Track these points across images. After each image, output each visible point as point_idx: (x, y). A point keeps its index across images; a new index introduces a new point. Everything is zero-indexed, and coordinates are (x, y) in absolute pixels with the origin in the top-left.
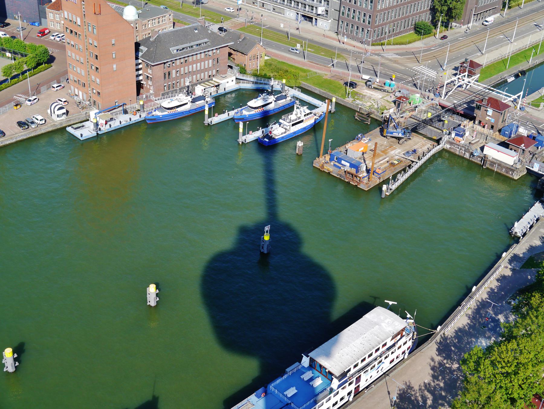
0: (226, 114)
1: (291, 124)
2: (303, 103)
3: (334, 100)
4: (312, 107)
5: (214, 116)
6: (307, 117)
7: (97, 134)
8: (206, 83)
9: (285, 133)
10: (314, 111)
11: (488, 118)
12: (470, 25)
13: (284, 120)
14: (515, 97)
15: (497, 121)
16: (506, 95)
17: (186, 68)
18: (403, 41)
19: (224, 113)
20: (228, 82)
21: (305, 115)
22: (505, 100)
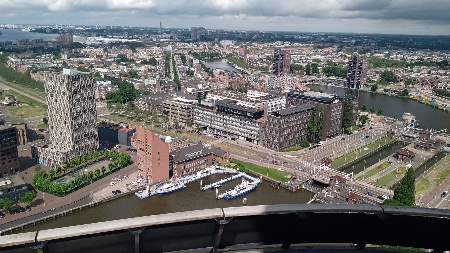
0: (211, 185)
1: (240, 189)
2: (246, 179)
3: (261, 177)
4: (251, 181)
5: (205, 186)
6: (248, 186)
7: (149, 196)
8: (202, 170)
9: (237, 193)
10: (252, 183)
11: (336, 185)
12: (327, 141)
13: (237, 187)
14: (349, 175)
15: (341, 187)
16: (344, 174)
17: (193, 164)
18: (294, 149)
19: (210, 184)
20: (212, 170)
21: (247, 185)
22: (344, 176)
